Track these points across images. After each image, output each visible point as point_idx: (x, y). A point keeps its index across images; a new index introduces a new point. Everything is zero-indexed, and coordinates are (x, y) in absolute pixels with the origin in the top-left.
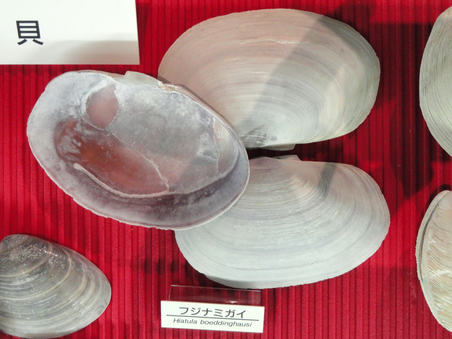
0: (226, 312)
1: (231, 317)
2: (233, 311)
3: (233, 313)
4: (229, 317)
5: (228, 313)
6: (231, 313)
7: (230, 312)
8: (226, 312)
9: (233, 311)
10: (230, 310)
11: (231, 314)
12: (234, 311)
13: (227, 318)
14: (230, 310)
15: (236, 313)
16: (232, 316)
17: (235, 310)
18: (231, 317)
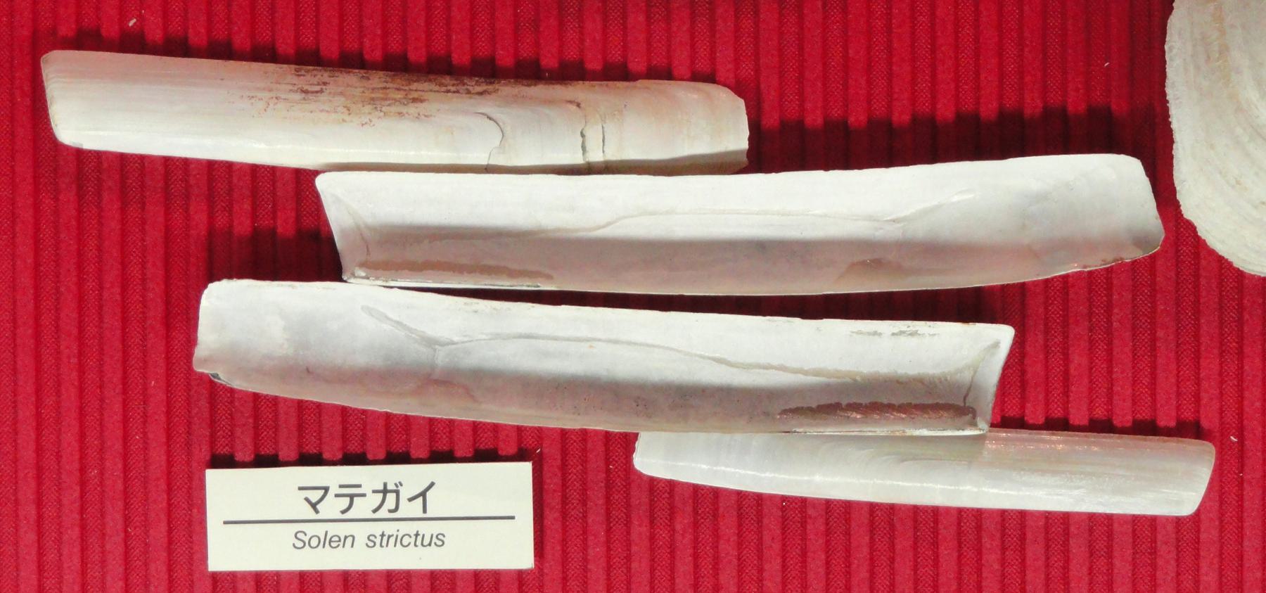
0: (374, 492)
1: (390, 511)
2: (396, 485)
3: (394, 495)
4: (383, 513)
5: (381, 495)
6: (389, 495)
7: (385, 491)
8: (374, 492)
9: (395, 488)
10: (385, 485)
11: (391, 498)
12: (400, 488)
13: (377, 515)
14: (385, 485)
15: (405, 495)
16: (393, 507)
17: (401, 485)
18: (390, 511)
